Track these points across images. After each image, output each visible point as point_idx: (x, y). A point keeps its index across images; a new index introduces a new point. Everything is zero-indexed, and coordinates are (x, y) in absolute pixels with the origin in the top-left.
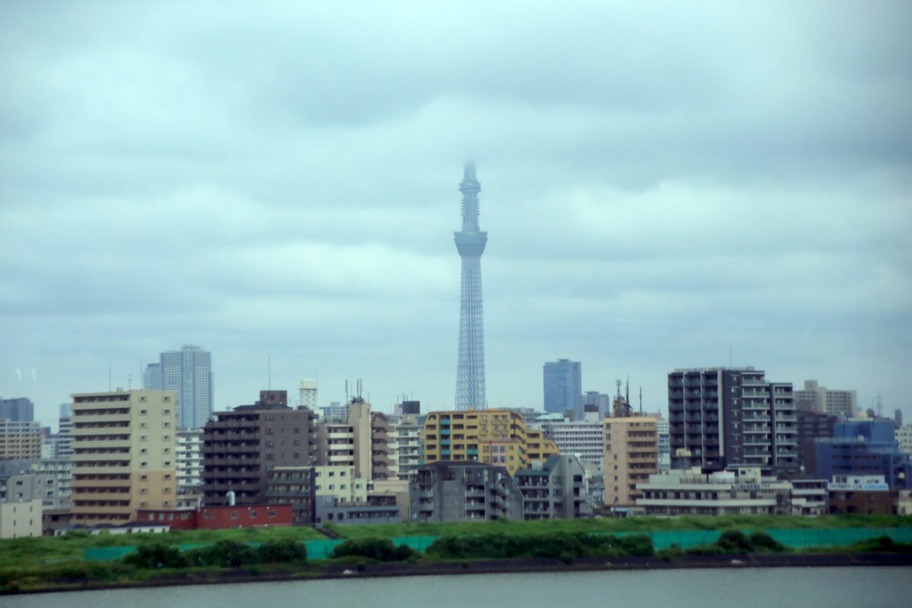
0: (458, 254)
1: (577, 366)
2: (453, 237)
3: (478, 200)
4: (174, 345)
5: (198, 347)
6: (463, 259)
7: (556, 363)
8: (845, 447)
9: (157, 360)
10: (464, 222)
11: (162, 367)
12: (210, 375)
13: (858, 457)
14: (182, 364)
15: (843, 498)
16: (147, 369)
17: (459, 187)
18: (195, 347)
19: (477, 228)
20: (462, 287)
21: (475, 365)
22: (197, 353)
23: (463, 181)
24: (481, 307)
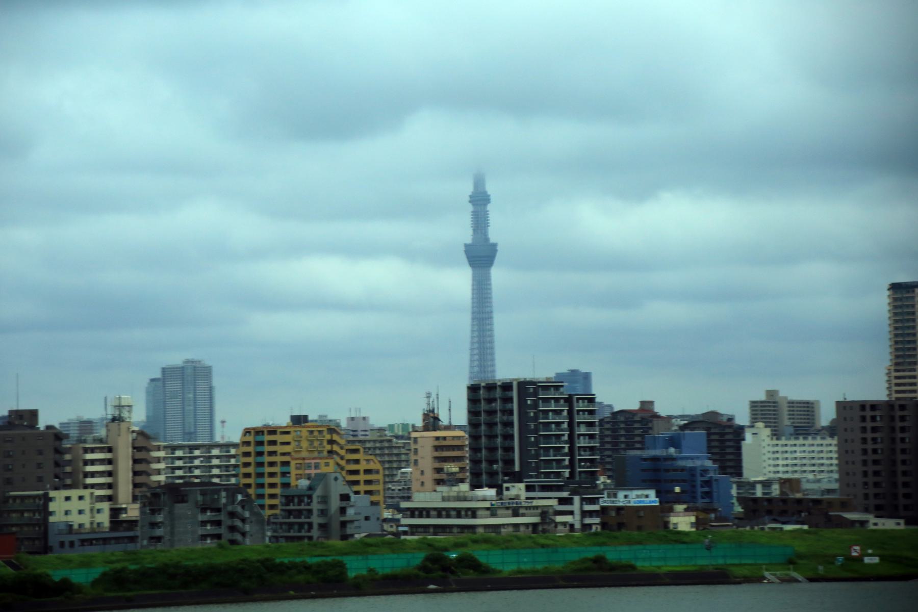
2: (463, 248)
3: (488, 211)
4: (176, 359)
5: (200, 361)
6: (473, 271)
8: (655, 459)
9: (158, 375)
11: (164, 382)
12: (211, 389)
13: (667, 471)
15: (613, 514)
16: (149, 384)
17: (468, 199)
18: (196, 361)
19: (487, 239)
20: (473, 298)
23: (473, 193)
24: (491, 318)
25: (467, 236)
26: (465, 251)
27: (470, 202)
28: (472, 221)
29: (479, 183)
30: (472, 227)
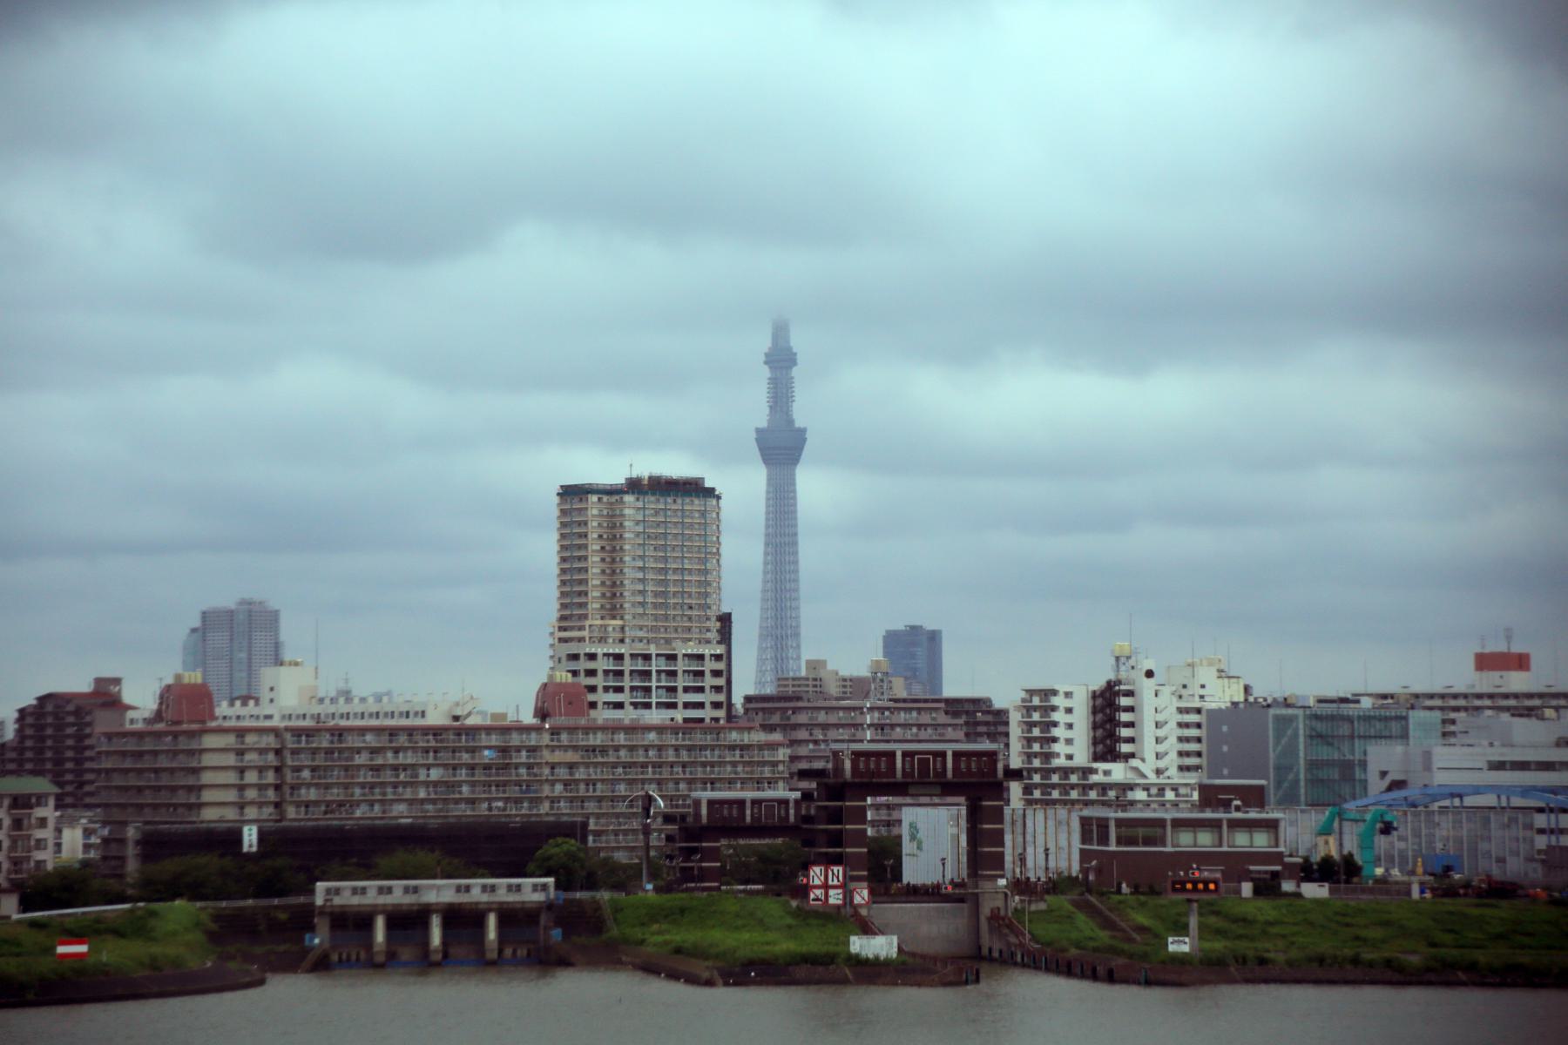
0: (761, 462)
1: (934, 638)
2: (754, 435)
3: (792, 378)
4: (226, 599)
5: (260, 603)
6: (768, 471)
7: (902, 631)
9: (197, 623)
10: (771, 412)
11: (204, 633)
14: (232, 628)
19: (791, 422)
21: (784, 633)
22: (256, 612)
23: (770, 349)
24: (795, 544)
25: (760, 416)
26: (756, 439)
27: (766, 363)
28: (768, 393)
29: (780, 332)
30: (768, 402)
